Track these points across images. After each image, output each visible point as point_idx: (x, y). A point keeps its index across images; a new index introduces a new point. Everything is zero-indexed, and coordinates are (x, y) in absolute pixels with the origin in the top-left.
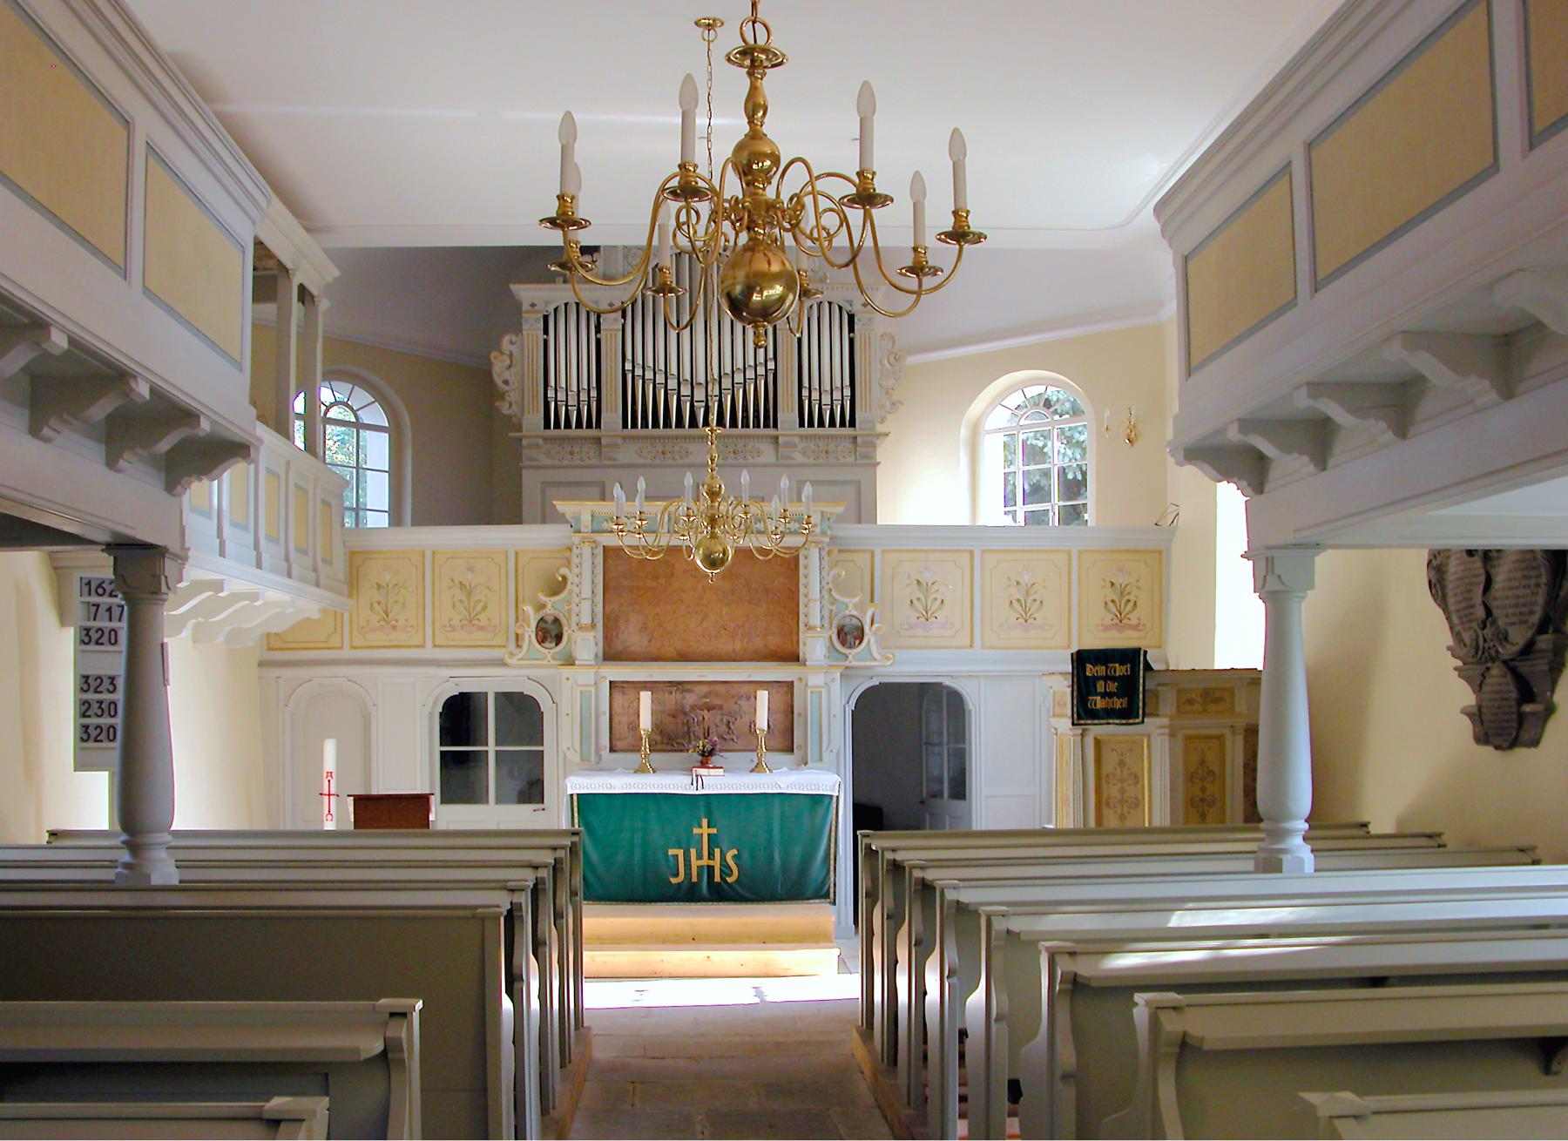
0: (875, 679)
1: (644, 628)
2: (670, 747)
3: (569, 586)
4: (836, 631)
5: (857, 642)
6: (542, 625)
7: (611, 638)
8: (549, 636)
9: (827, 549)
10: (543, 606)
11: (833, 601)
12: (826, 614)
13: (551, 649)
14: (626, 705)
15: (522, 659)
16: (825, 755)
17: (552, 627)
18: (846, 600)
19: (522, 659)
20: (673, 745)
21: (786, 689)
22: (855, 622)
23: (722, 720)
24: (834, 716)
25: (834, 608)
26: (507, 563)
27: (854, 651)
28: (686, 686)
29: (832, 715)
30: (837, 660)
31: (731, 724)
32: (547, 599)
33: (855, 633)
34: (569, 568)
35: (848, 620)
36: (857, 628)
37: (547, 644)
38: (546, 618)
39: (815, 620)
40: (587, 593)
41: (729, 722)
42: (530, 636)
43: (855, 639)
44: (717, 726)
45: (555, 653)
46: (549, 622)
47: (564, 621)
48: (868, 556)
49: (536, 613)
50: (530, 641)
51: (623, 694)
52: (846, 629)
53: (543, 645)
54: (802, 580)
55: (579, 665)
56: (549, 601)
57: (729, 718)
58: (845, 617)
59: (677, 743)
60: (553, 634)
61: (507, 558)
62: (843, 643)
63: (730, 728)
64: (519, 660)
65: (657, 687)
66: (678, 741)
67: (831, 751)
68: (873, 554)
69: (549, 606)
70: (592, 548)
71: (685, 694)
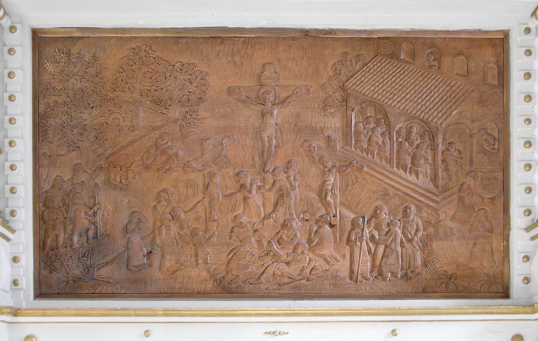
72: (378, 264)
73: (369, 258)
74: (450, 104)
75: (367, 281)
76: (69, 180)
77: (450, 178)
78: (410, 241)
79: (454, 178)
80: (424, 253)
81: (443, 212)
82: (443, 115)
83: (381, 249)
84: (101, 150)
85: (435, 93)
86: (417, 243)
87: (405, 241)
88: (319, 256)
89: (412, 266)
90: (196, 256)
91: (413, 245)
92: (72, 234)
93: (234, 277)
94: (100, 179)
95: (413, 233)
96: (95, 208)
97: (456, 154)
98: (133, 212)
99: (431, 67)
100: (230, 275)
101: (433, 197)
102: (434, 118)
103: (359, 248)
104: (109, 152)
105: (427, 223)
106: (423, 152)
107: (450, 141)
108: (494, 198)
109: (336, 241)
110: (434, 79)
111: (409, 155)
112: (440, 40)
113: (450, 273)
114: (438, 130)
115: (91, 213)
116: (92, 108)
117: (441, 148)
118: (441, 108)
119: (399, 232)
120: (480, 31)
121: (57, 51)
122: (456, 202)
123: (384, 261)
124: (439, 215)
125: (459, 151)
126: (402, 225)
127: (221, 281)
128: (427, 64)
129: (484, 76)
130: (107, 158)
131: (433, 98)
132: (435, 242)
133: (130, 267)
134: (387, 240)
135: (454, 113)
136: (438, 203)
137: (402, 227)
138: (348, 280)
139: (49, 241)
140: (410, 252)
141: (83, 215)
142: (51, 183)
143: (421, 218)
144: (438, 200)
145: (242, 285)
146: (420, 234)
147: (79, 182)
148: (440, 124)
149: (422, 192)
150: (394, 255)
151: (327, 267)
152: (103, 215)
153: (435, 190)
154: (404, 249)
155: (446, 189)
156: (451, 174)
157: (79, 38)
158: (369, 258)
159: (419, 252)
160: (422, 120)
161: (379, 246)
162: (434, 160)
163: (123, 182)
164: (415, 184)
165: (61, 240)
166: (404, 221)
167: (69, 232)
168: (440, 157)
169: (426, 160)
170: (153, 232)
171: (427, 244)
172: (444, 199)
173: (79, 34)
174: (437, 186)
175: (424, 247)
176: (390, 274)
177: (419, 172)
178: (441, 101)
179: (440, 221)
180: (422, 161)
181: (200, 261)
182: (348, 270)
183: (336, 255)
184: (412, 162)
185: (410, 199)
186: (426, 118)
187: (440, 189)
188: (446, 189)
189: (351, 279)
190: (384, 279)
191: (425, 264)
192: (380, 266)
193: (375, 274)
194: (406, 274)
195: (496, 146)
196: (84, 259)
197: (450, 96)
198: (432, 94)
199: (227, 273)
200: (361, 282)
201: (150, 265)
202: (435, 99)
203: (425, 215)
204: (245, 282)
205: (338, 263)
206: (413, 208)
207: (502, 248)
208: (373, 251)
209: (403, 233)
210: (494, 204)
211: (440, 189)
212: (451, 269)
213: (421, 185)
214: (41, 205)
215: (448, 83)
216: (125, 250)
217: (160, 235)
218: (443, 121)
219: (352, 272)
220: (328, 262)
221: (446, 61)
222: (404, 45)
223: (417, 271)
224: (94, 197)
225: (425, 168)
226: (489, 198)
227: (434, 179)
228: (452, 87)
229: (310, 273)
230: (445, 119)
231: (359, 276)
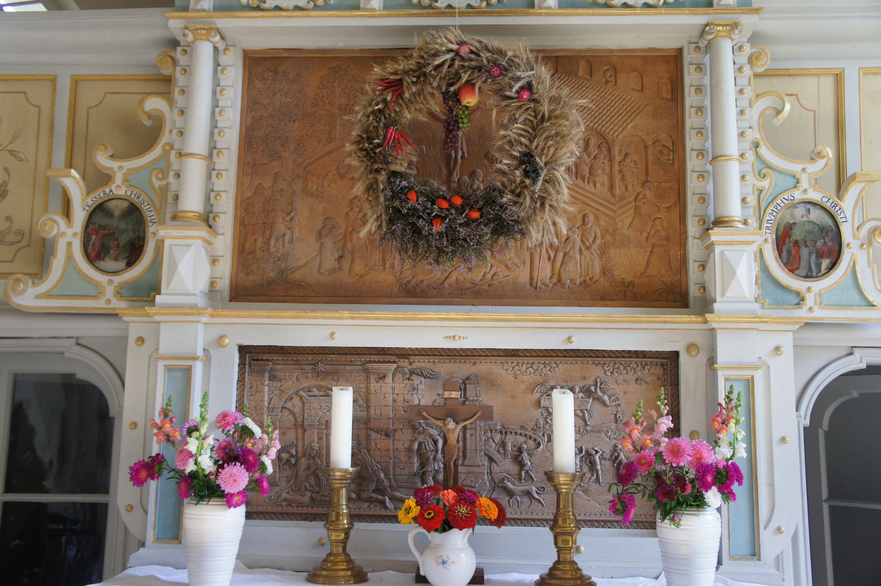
0: (858, 353)
1: (326, 229)
2: (378, 511)
3: (165, 138)
4: (771, 237)
5: (825, 263)
6: (101, 220)
7: (252, 252)
8: (112, 244)
9: (748, 50)
10: (106, 178)
11: (764, 169)
12: (752, 200)
13: (115, 273)
14: (277, 403)
15: (48, 295)
16: (766, 536)
17: (122, 226)
18: (795, 167)
19: (48, 295)
20: (383, 503)
21: (659, 371)
22: (816, 215)
23: (503, 444)
24: (783, 440)
25: (765, 184)
26: (53, 104)
27: (817, 286)
28: (419, 363)
29: (776, 438)
30: (778, 304)
31: (525, 455)
32: (114, 164)
33: (819, 244)
34: (167, 95)
35: (800, 212)
36: (822, 229)
37: (109, 264)
38: (112, 204)
39: (734, 209)
40: (198, 141)
41: (520, 451)
42: (69, 244)
43: (820, 255)
44: (491, 460)
45: (122, 286)
46: (117, 213)
47: (149, 213)
48: (828, 84)
49: (88, 193)
50: (70, 257)
51: (272, 378)
52: (797, 234)
53: (102, 264)
54: (691, 120)
55: (165, 307)
56: (120, 169)
57: (522, 439)
58: (794, 206)
59: (392, 499)
60: (124, 239)
61: (54, 91)
62: (791, 264)
63: (522, 465)
64: (38, 297)
65: (351, 363)
66: (398, 494)
67: (779, 530)
68: (839, 79)
69: (119, 179)
70: (216, 49)
71: (417, 380)
72: (557, 270)
73: (548, 265)
74: (625, 118)
75: (546, 288)
76: (269, 187)
77: (626, 188)
78: (588, 248)
79: (630, 187)
80: (602, 261)
81: (621, 220)
82: (619, 127)
83: (560, 256)
84: (300, 160)
85: (611, 107)
86: (595, 250)
87: (583, 249)
88: (501, 261)
89: (590, 273)
90: (384, 260)
91: (591, 253)
92: (269, 239)
93: (419, 281)
94: (298, 187)
95: (591, 240)
96: (292, 214)
97: (632, 165)
98: (327, 218)
99: (607, 82)
100: (415, 280)
101: (611, 206)
102: (611, 130)
103: (539, 255)
104: (308, 161)
105: (605, 231)
106: (601, 162)
107: (627, 152)
109: (517, 247)
110: (610, 94)
111: (587, 166)
112: (616, 58)
113: (627, 280)
114: (614, 141)
115: (288, 218)
116: (294, 121)
117: (618, 158)
118: (617, 121)
119: (578, 239)
120: (654, 50)
121: (265, 70)
122: (633, 211)
123: (563, 268)
124: (616, 223)
125: (635, 161)
126: (581, 233)
127: (406, 286)
128: (604, 80)
129: (658, 90)
130: (305, 167)
131: (609, 112)
132: (612, 250)
133: (322, 271)
134: (566, 248)
135: (629, 126)
136: (615, 211)
137: (580, 235)
138: (528, 286)
139: (248, 245)
140: (589, 259)
141: (280, 220)
142: (253, 190)
143: (599, 226)
144: (615, 209)
145: (426, 290)
146: (598, 242)
147: (279, 190)
148: (617, 136)
149: (600, 201)
150: (573, 262)
151: (508, 273)
152: (299, 221)
153: (612, 200)
154: (583, 256)
155: (622, 198)
156: (627, 184)
157: (285, 58)
158: (548, 264)
159: (597, 260)
160: (597, 133)
161: (558, 253)
162: (611, 170)
163: (319, 189)
164: (594, 194)
165: (259, 244)
166: (583, 229)
167: (267, 236)
168: (616, 168)
169: (604, 170)
170: (345, 237)
171: (604, 252)
172: (621, 208)
173: (286, 55)
174: (613, 195)
175: (601, 254)
176: (569, 281)
177: (597, 181)
178: (617, 115)
179: (617, 229)
180: (599, 171)
181: (388, 265)
182: (528, 277)
183: (516, 261)
184: (590, 173)
185: (588, 208)
186: (602, 130)
187: (617, 198)
188: (622, 198)
189: (531, 285)
190: (563, 286)
191: (604, 271)
192: (559, 273)
193: (555, 280)
194: (585, 281)
195: (671, 158)
196: (279, 262)
197: (626, 109)
198: (608, 108)
199: (413, 277)
200: (540, 288)
201: (340, 269)
202: (612, 112)
203: (603, 223)
204: (428, 286)
205: (519, 270)
206: (591, 217)
207: (679, 257)
208: (552, 258)
209: (582, 241)
210: (670, 213)
211: (617, 198)
212: (628, 278)
213: (598, 195)
214: (243, 210)
215: (623, 97)
216: (318, 255)
217: (351, 240)
218: (619, 133)
219: (531, 278)
220: (508, 268)
221: (622, 78)
222: (582, 64)
223: (595, 279)
224: (292, 204)
225: (602, 179)
226: (665, 208)
227: (611, 188)
228: (628, 101)
229: (492, 279)
230: (621, 132)
231: (539, 283)
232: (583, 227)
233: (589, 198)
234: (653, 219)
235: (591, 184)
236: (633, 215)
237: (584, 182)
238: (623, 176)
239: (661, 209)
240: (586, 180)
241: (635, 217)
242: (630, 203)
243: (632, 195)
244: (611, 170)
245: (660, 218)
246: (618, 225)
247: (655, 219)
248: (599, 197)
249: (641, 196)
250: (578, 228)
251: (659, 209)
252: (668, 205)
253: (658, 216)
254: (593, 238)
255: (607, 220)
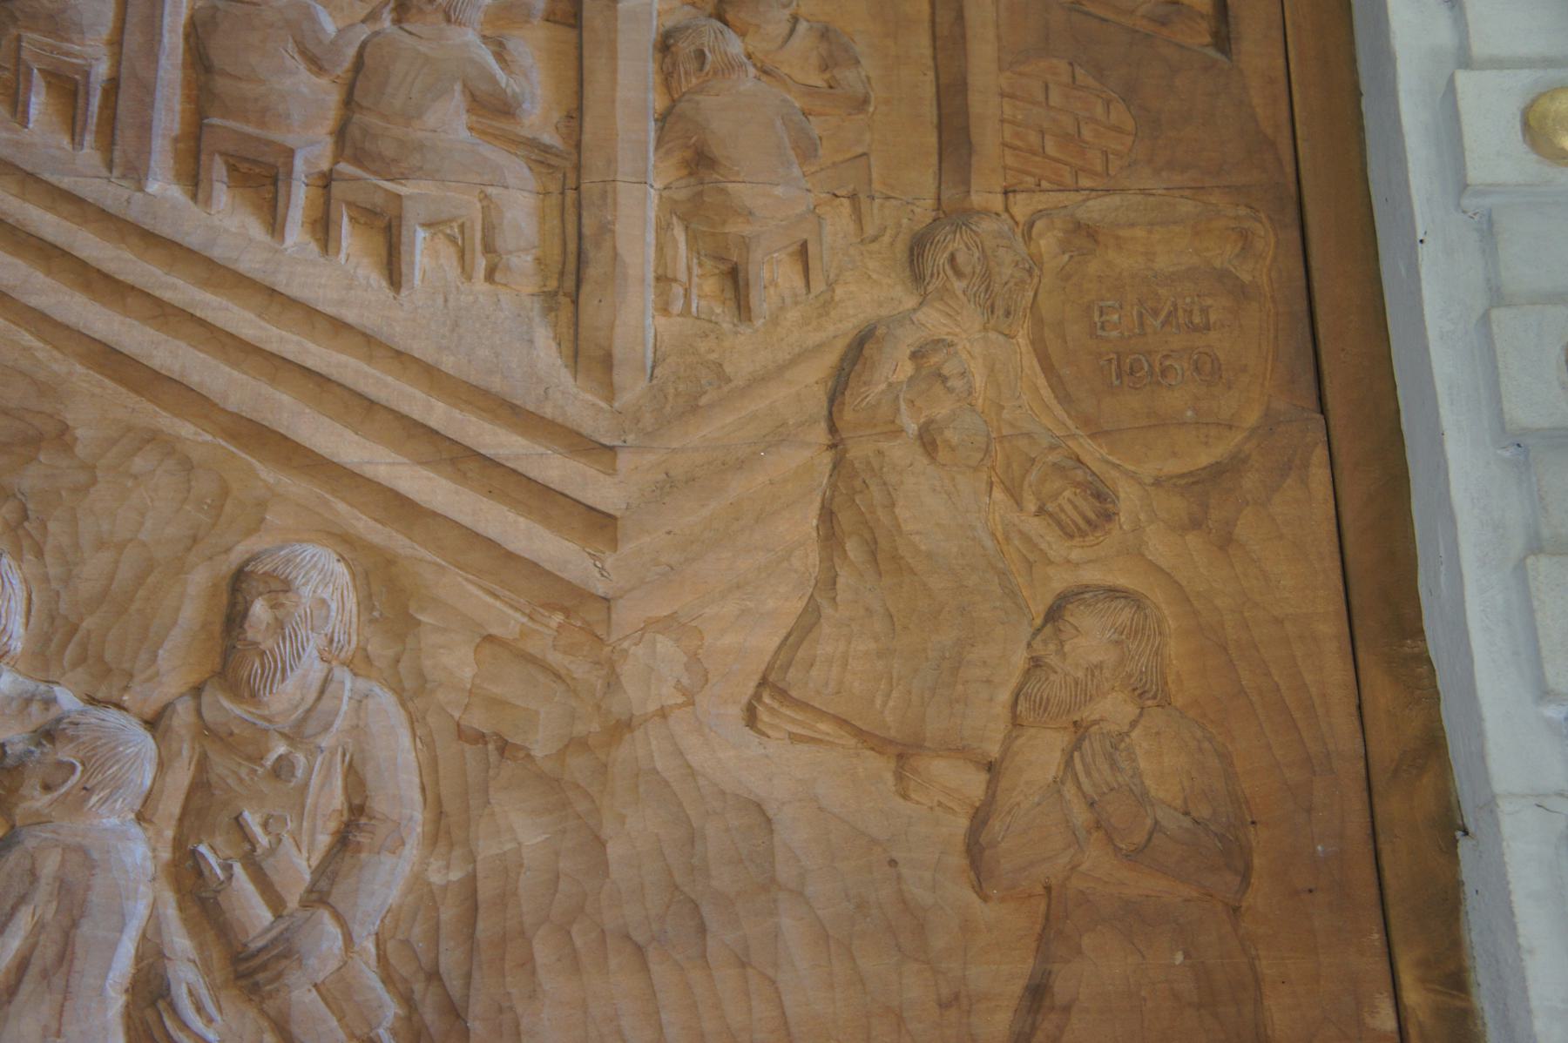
77: (735, 280)
87: (186, 976)
108: (1217, 472)
126: (181, 776)
137: (171, 805)
144: (603, 492)
149: (437, 413)
156: (745, 244)
162: (575, 116)
164: (369, 343)
166: (205, 731)
177: (413, 215)
179: (622, 727)
184: (341, 134)
187: (632, 388)
213: (421, 348)
232: (224, 708)
233: (318, 383)
234: (1039, 609)
235: (347, 233)
236: (810, 559)
237: (275, 225)
238: (700, 161)
239: (1128, 498)
240: (300, 197)
241: (829, 582)
242: (779, 436)
243: (802, 356)
244: (575, 116)
245: (1113, 593)
246: (627, 671)
247: (1054, 614)
248: (430, 376)
249: (893, 366)
250: (153, 724)
251: (1101, 495)
252: (1204, 459)
253: (1092, 575)
254: (324, 840)
255: (508, 620)
